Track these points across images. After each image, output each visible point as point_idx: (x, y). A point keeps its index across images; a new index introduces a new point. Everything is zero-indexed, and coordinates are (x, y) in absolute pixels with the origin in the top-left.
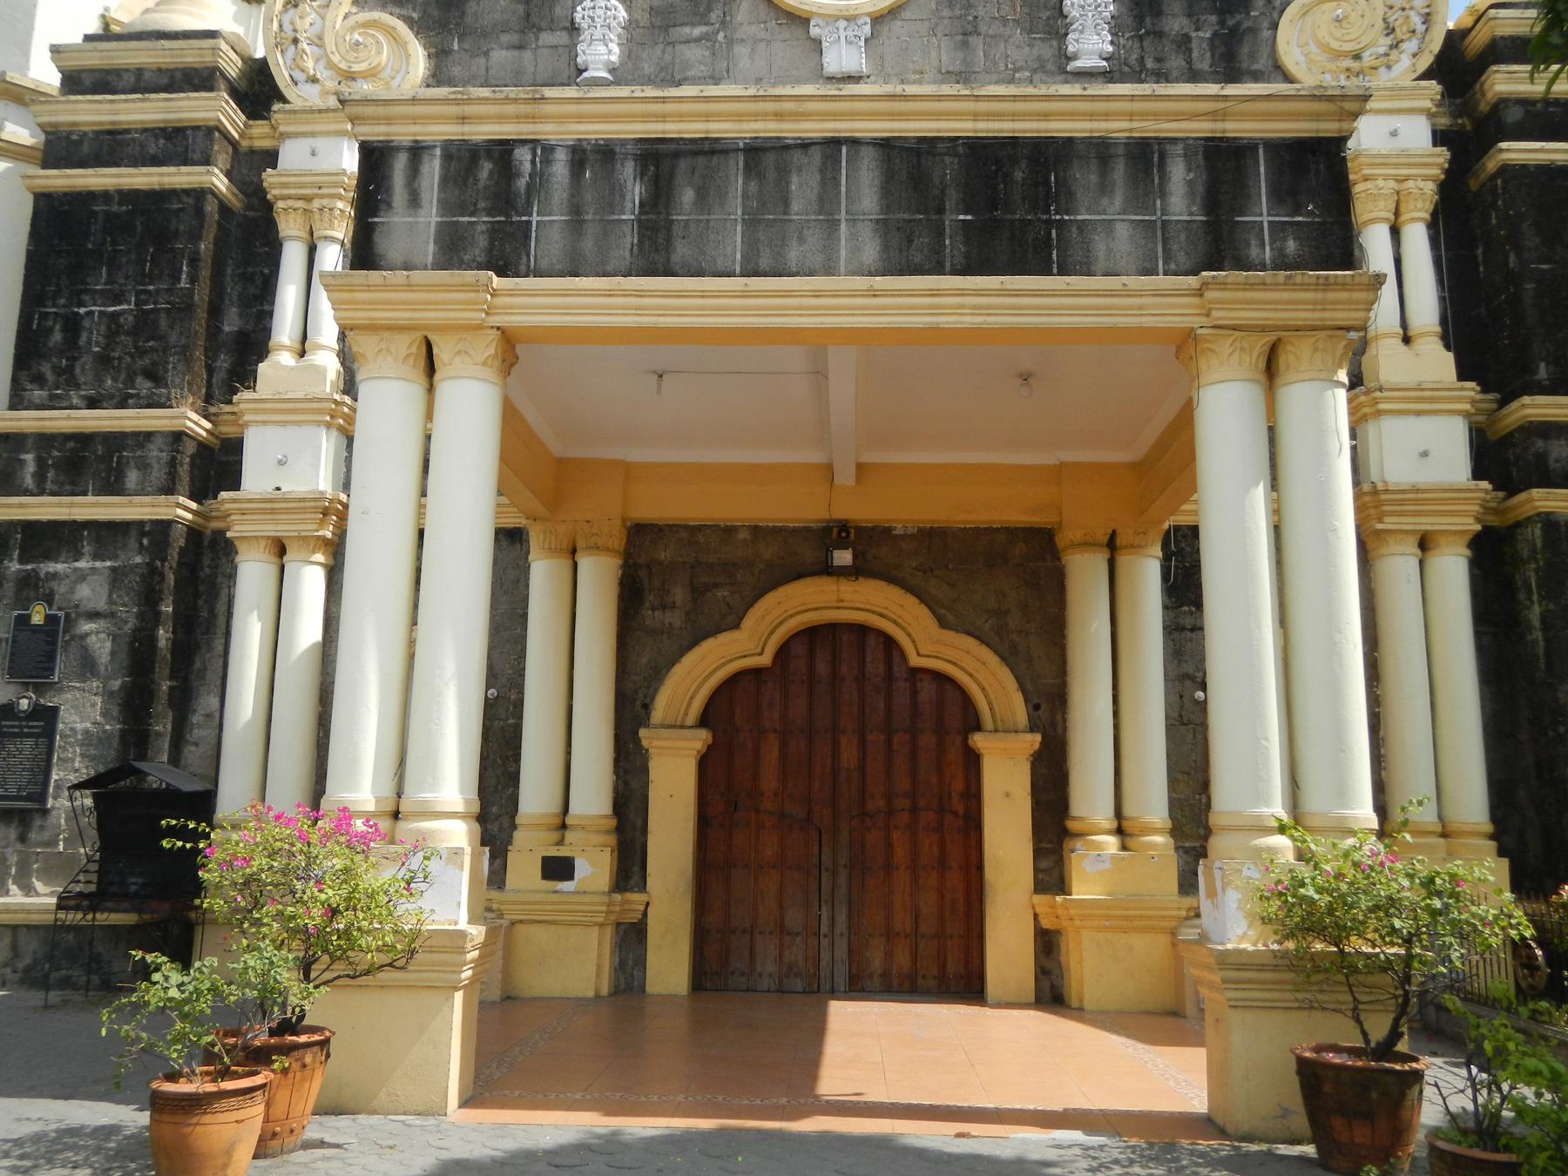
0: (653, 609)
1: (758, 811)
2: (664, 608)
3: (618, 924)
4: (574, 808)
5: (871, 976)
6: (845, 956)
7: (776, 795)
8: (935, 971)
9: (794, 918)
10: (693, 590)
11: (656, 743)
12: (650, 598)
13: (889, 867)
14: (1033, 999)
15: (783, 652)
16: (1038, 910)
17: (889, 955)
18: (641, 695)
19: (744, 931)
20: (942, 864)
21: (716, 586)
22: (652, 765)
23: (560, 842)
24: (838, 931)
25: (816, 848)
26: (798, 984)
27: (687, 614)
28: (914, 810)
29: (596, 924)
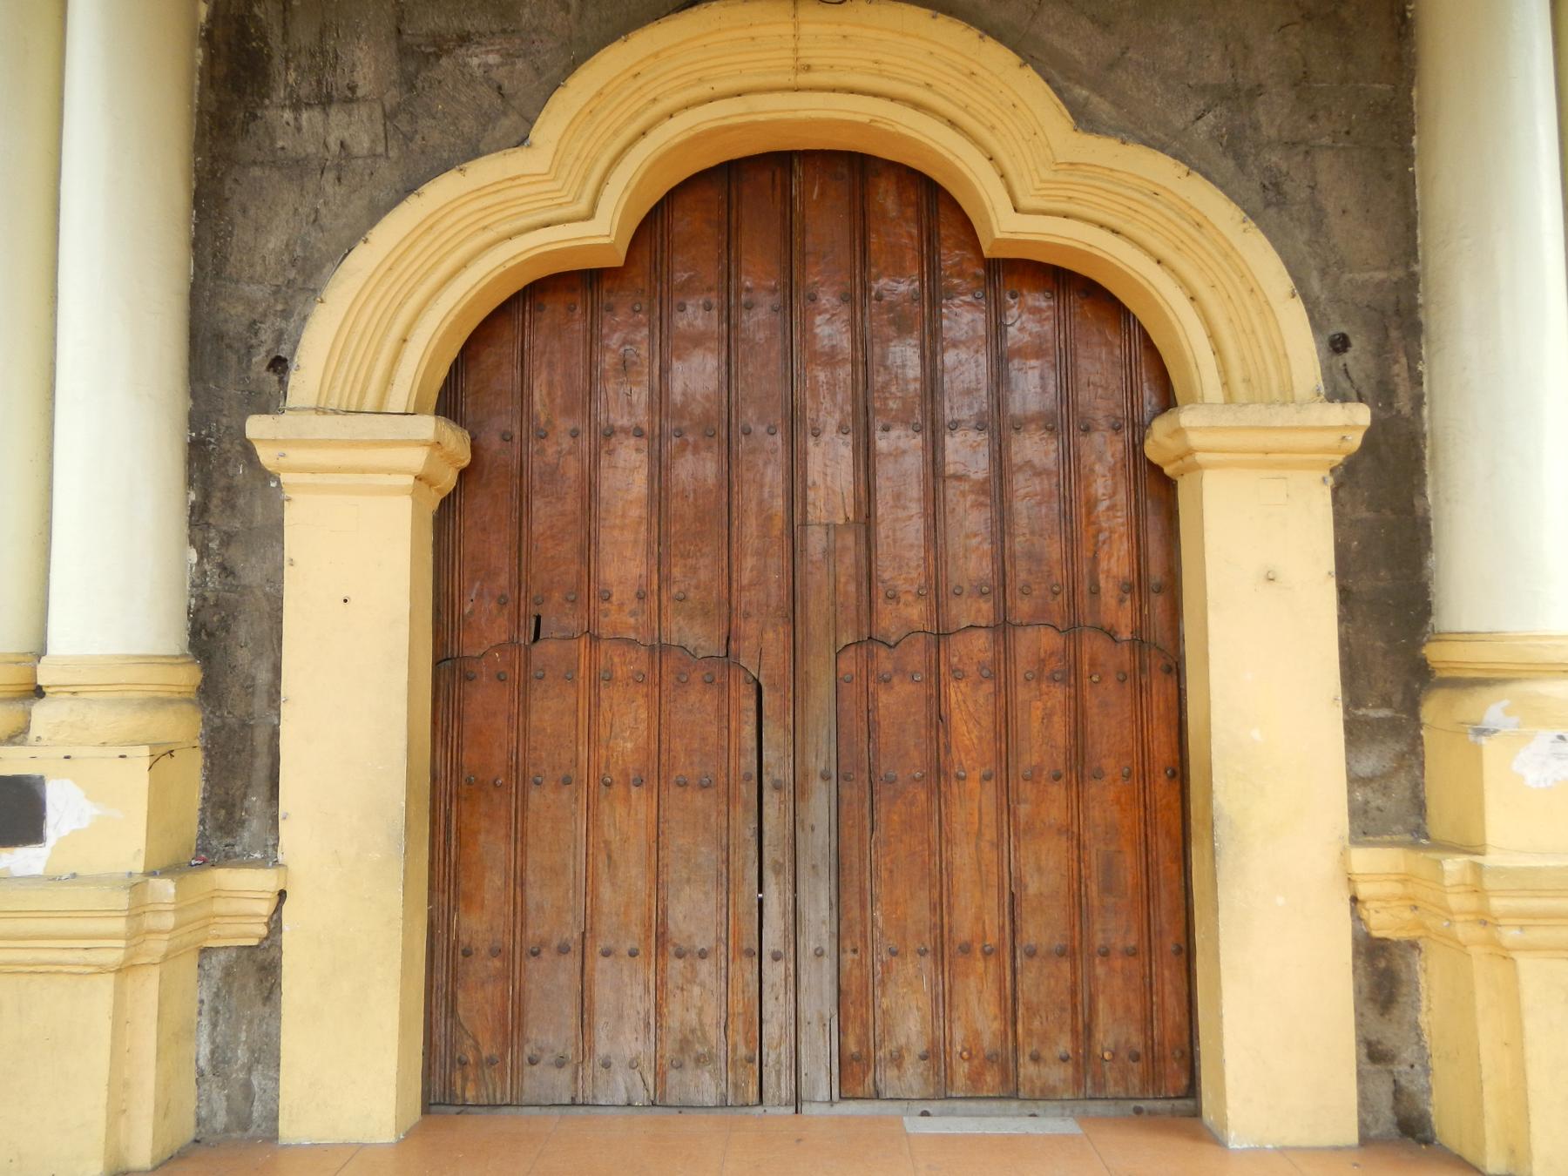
0: (296, 107)
1: (595, 639)
2: (325, 101)
3: (205, 952)
4: (61, 642)
5: (897, 1060)
6: (829, 1008)
7: (641, 597)
8: (1064, 1045)
9: (694, 913)
10: (405, 53)
11: (297, 456)
12: (287, 79)
13: (938, 774)
14: (1352, 1137)
15: (654, 227)
16: (1363, 891)
17: (944, 1003)
18: (266, 335)
19: (563, 950)
20: (1078, 765)
21: (464, 39)
22: (290, 515)
23: (18, 736)
24: (808, 943)
25: (749, 730)
26: (706, 1086)
27: (389, 116)
28: (1003, 627)
29: (102, 969)
